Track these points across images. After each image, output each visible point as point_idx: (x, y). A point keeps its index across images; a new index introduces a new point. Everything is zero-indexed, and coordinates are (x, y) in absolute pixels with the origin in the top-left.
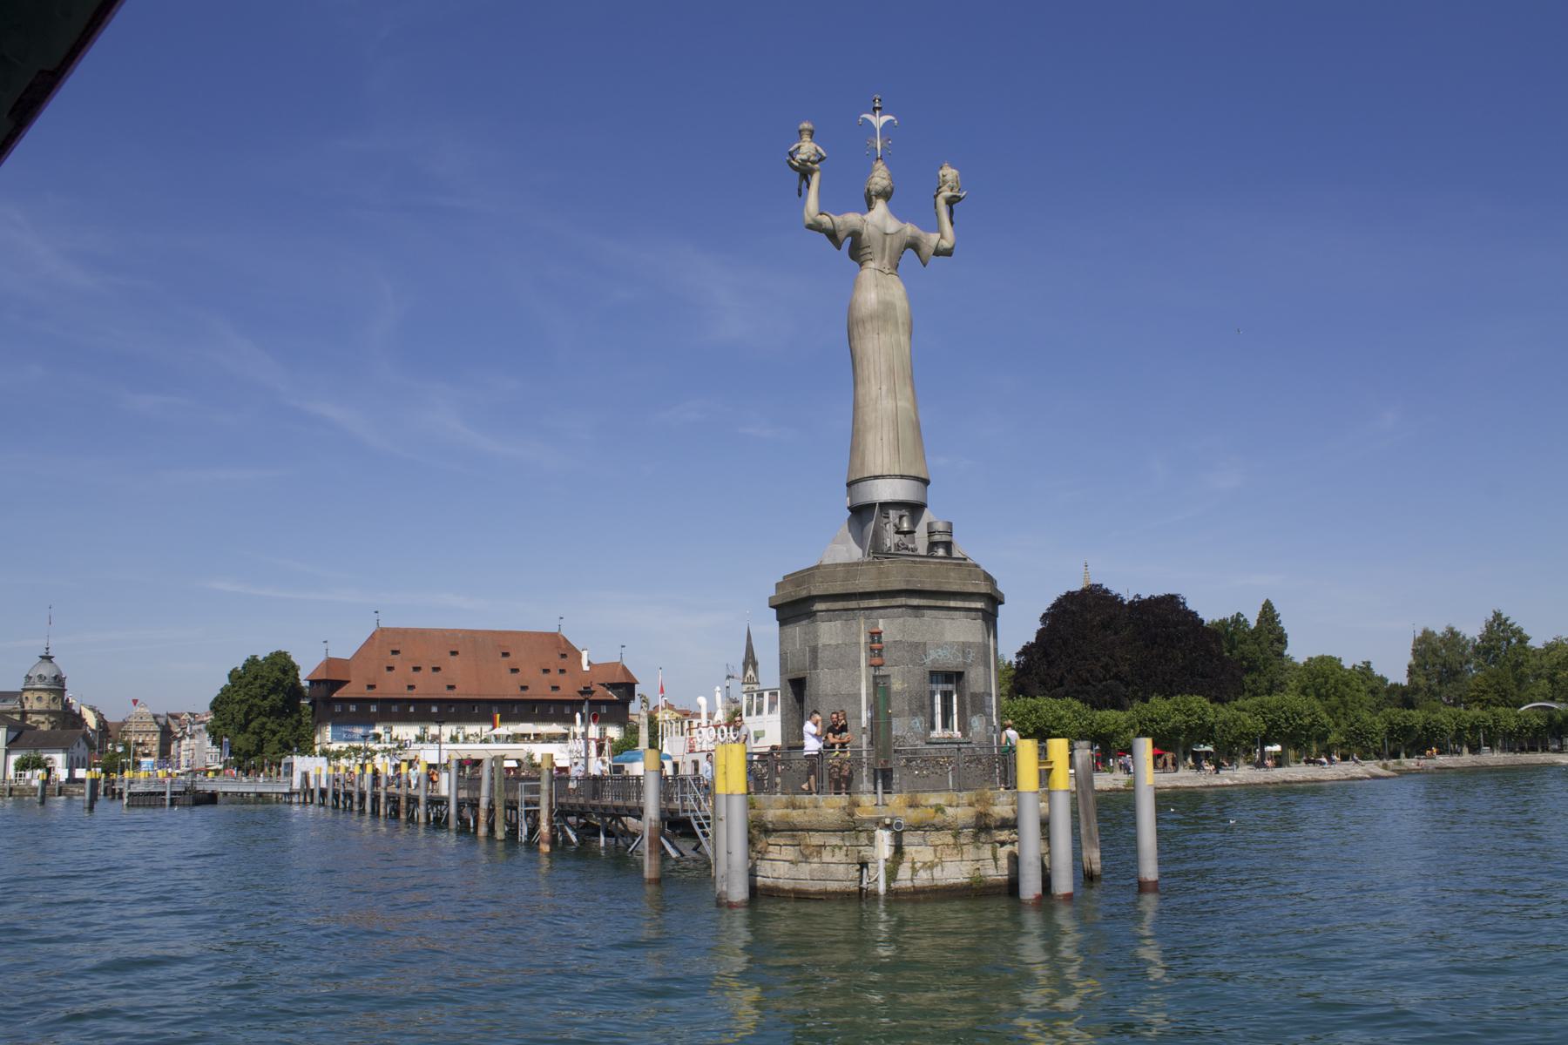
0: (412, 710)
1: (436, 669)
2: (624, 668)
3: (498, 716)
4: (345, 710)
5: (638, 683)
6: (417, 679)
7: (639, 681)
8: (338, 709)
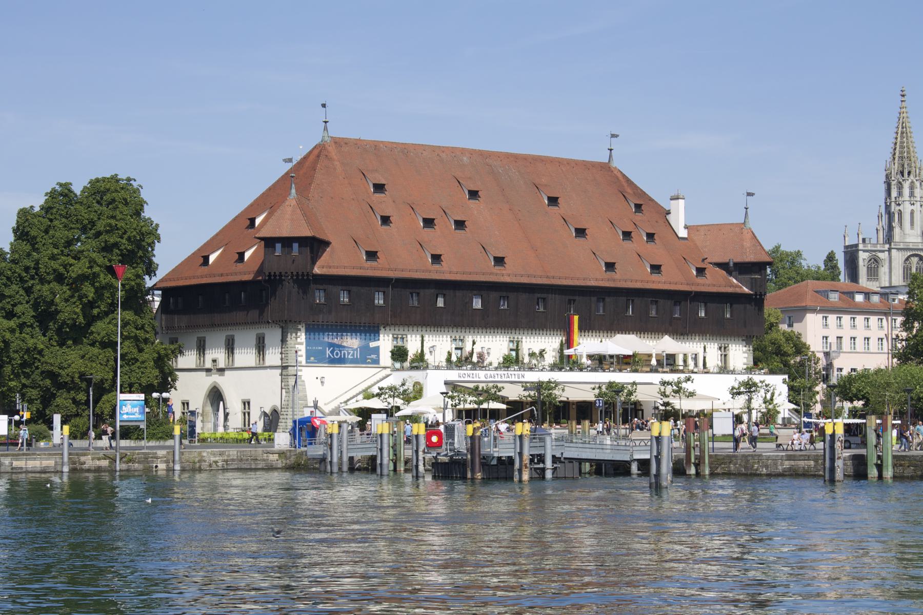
0: (440, 303)
3: (576, 318)
6: (438, 239)
8: (319, 298)
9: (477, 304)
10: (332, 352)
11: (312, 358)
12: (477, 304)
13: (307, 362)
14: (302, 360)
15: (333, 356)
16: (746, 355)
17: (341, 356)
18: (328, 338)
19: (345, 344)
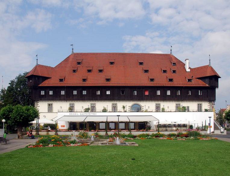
1: (101, 71)
2: (212, 68)
4: (47, 93)
5: (220, 78)
7: (220, 76)
8: (43, 93)
9: (99, 93)
16: (209, 107)
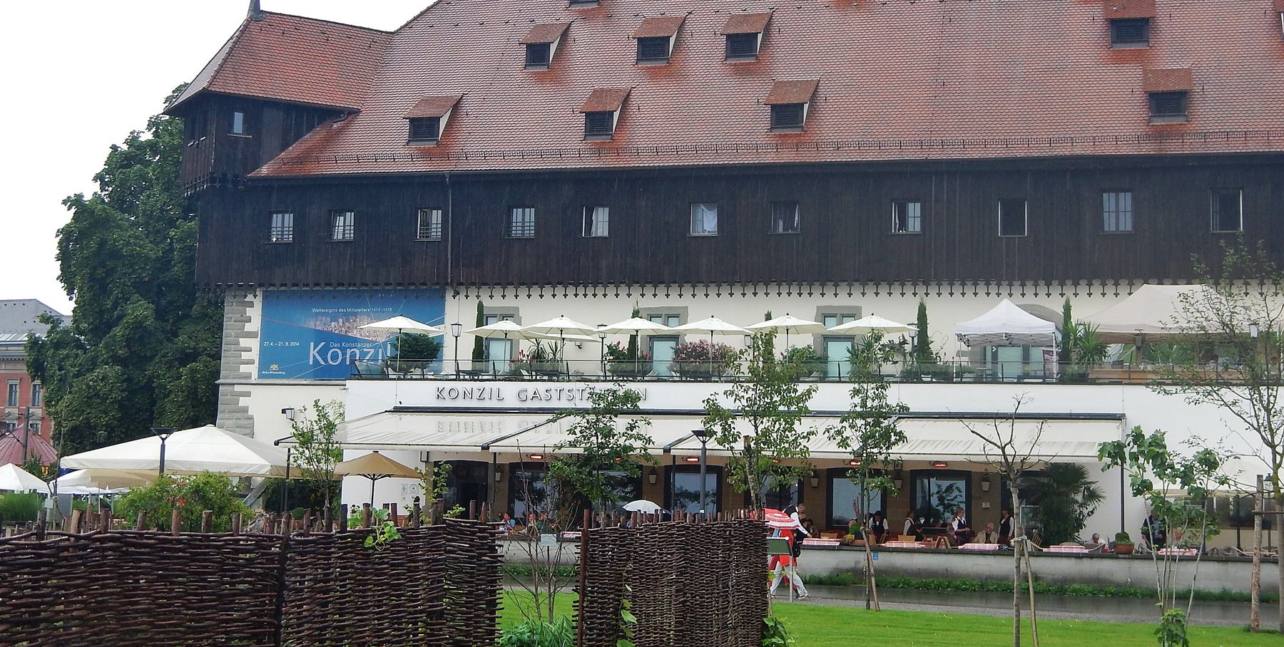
9: (707, 222)
10: (323, 353)
11: (274, 367)
12: (707, 222)
13: (260, 376)
14: (253, 370)
15: (325, 360)
17: (344, 360)
18: (317, 319)
19: (355, 334)
